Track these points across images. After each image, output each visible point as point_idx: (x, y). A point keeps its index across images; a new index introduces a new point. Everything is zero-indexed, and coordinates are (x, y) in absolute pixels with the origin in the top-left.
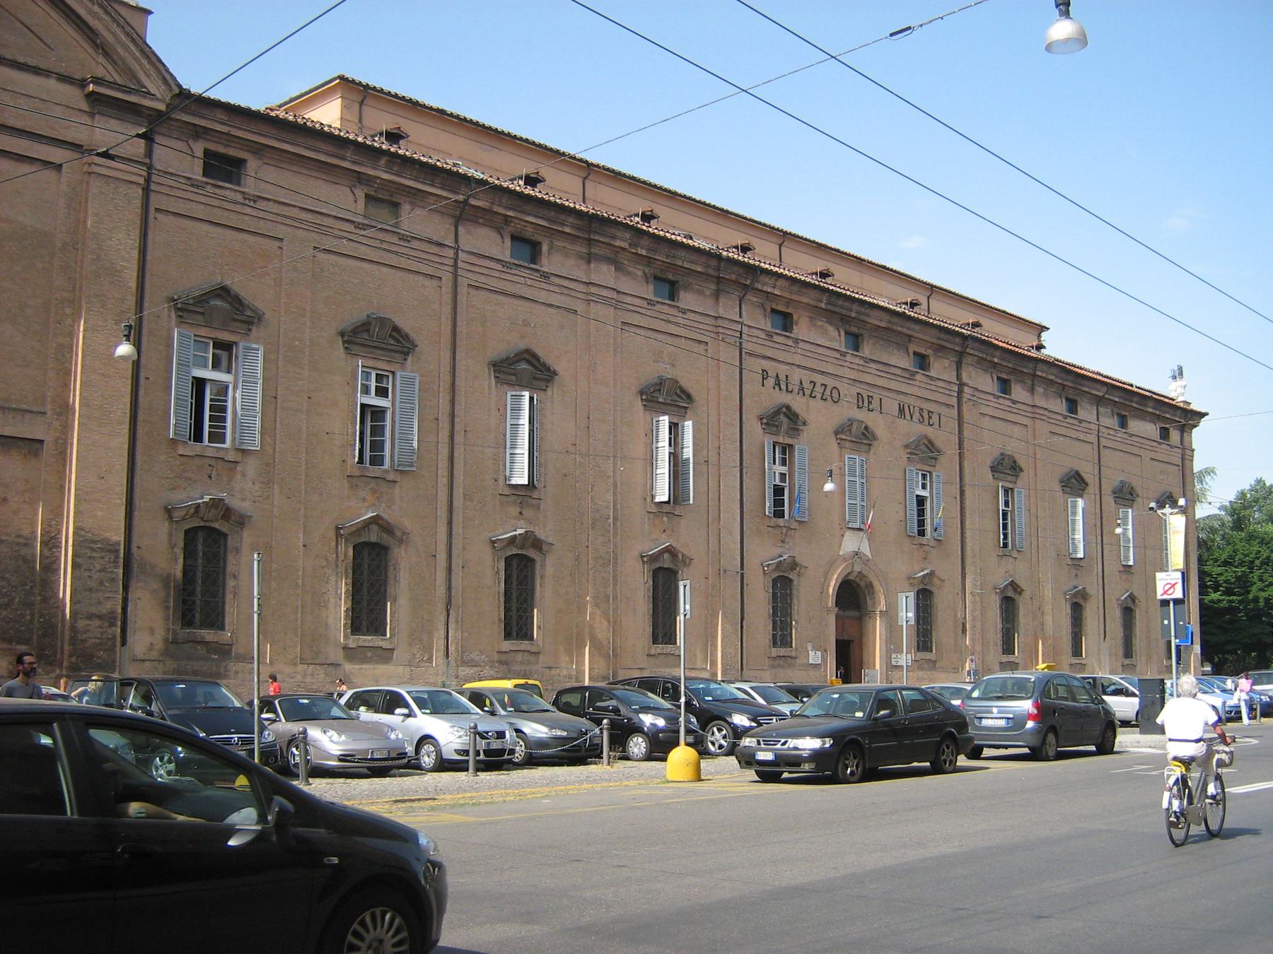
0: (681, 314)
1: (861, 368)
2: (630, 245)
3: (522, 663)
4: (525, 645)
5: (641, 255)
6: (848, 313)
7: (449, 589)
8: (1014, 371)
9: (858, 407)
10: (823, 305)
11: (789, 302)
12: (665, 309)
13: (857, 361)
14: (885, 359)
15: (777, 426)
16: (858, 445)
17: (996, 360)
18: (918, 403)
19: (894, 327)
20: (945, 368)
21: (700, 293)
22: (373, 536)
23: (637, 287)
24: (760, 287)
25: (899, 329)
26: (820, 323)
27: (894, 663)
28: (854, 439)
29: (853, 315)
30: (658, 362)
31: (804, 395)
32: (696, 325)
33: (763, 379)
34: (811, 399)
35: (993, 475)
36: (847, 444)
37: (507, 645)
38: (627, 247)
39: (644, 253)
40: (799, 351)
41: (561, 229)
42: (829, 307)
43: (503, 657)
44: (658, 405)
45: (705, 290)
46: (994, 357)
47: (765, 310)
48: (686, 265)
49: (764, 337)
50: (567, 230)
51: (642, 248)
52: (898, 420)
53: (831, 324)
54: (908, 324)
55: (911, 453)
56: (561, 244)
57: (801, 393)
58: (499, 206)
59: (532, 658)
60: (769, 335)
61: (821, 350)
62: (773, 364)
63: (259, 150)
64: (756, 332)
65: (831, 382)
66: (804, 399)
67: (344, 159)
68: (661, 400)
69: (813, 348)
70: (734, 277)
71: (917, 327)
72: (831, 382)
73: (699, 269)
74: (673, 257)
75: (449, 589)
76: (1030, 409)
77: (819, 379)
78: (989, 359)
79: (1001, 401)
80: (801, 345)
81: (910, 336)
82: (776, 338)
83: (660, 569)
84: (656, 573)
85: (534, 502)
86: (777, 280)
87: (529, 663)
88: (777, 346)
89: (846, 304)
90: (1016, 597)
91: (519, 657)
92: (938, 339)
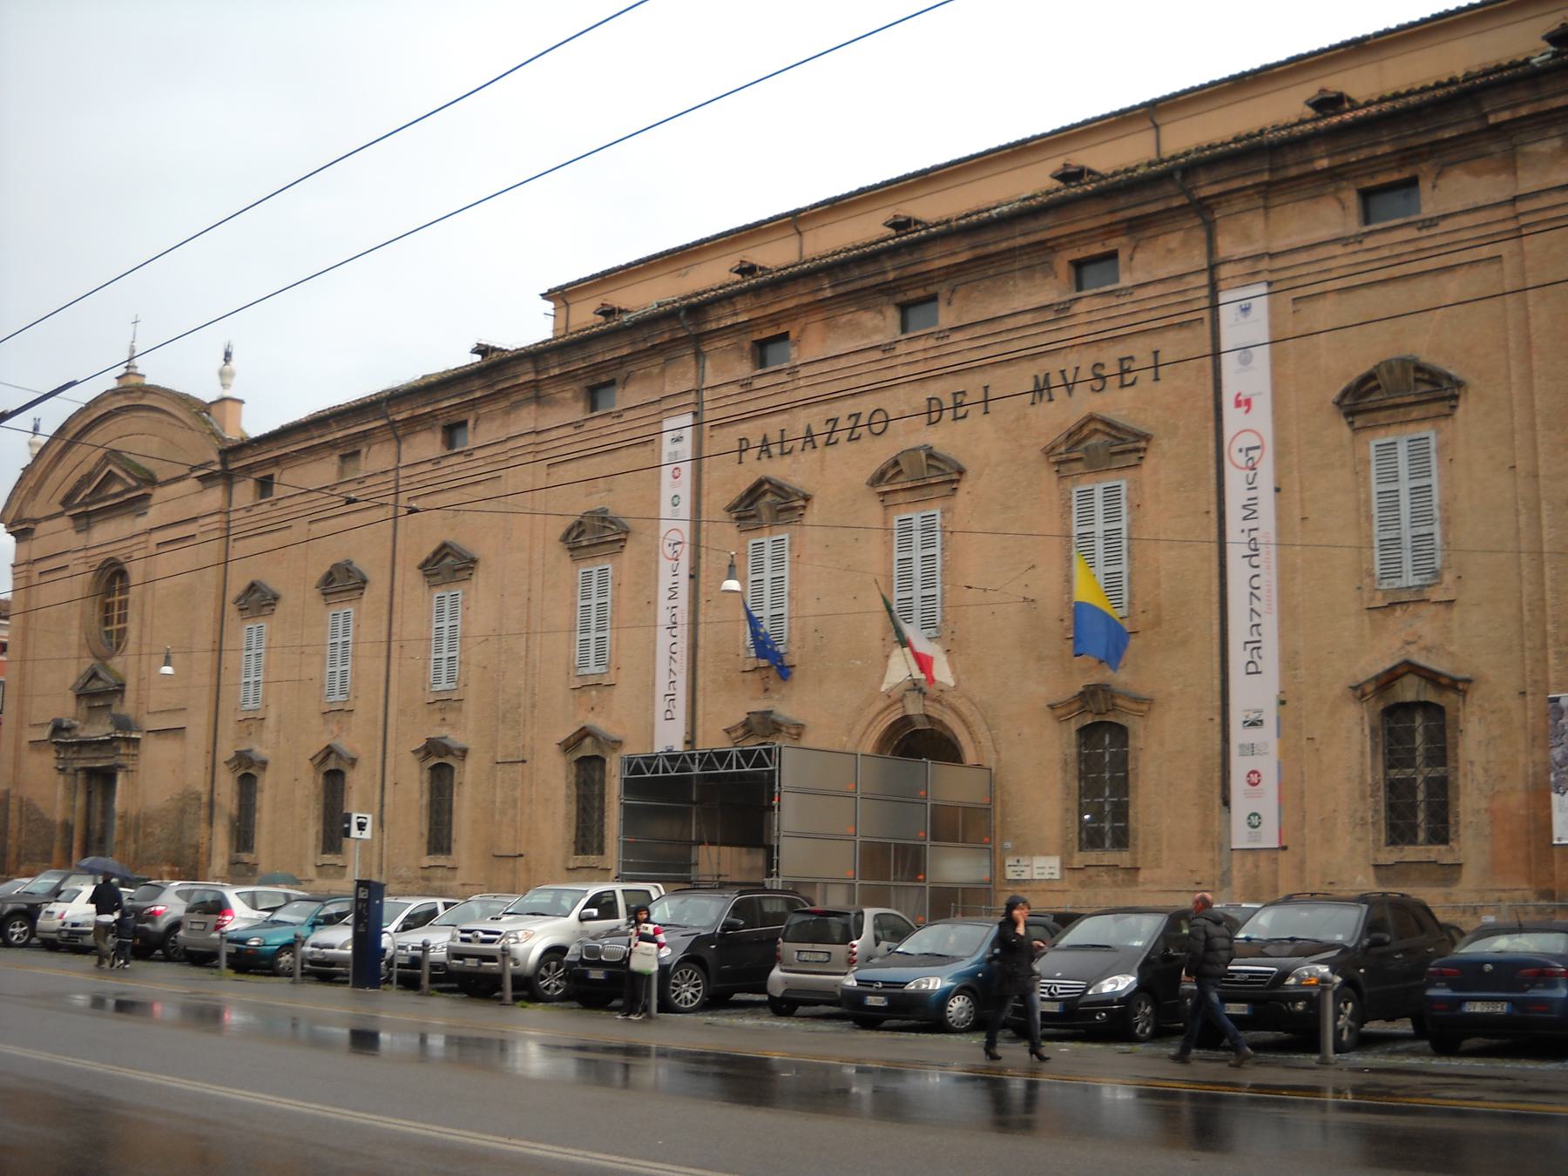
1: (932, 353)
2: (537, 372)
3: (442, 879)
4: (441, 860)
5: (555, 376)
6: (880, 279)
7: (382, 806)
8: (1409, 156)
9: (930, 424)
10: (828, 293)
11: (773, 319)
12: (597, 423)
13: (920, 345)
14: (996, 308)
15: (754, 516)
16: (926, 491)
17: (1324, 163)
18: (1085, 359)
19: (992, 249)
20: (1170, 251)
21: (647, 376)
22: (1409, 690)
23: (568, 409)
24: (714, 326)
25: (1004, 245)
26: (844, 319)
27: (1010, 875)
28: (909, 485)
29: (891, 276)
30: (592, 493)
31: (814, 447)
34: (828, 449)
35: (1351, 423)
36: (900, 498)
37: (427, 861)
38: (531, 377)
39: (557, 371)
40: (802, 383)
41: (471, 397)
42: (841, 290)
43: (426, 873)
44: (585, 550)
46: (1311, 160)
47: (741, 349)
48: (608, 357)
50: (478, 395)
51: (553, 367)
52: (1033, 409)
53: (866, 309)
54: (1019, 228)
55: (1059, 463)
56: (486, 410)
57: (810, 445)
58: (418, 407)
59: (450, 874)
60: (746, 384)
61: (843, 362)
62: (760, 422)
63: (276, 461)
64: (724, 391)
65: (866, 405)
66: (816, 454)
67: (313, 438)
68: (584, 543)
69: (825, 367)
70: (667, 337)
71: (1047, 221)
72: (866, 405)
73: (625, 351)
74: (590, 356)
75: (382, 806)
76: (1505, 212)
77: (843, 410)
78: (1293, 172)
79: (1369, 243)
80: (804, 372)
81: (1042, 242)
82: (758, 383)
83: (584, 758)
84: (583, 762)
85: (457, 704)
86: (734, 304)
87: (447, 879)
88: (762, 393)
89: (871, 268)
90: (1447, 700)
91: (439, 872)
92: (1111, 212)
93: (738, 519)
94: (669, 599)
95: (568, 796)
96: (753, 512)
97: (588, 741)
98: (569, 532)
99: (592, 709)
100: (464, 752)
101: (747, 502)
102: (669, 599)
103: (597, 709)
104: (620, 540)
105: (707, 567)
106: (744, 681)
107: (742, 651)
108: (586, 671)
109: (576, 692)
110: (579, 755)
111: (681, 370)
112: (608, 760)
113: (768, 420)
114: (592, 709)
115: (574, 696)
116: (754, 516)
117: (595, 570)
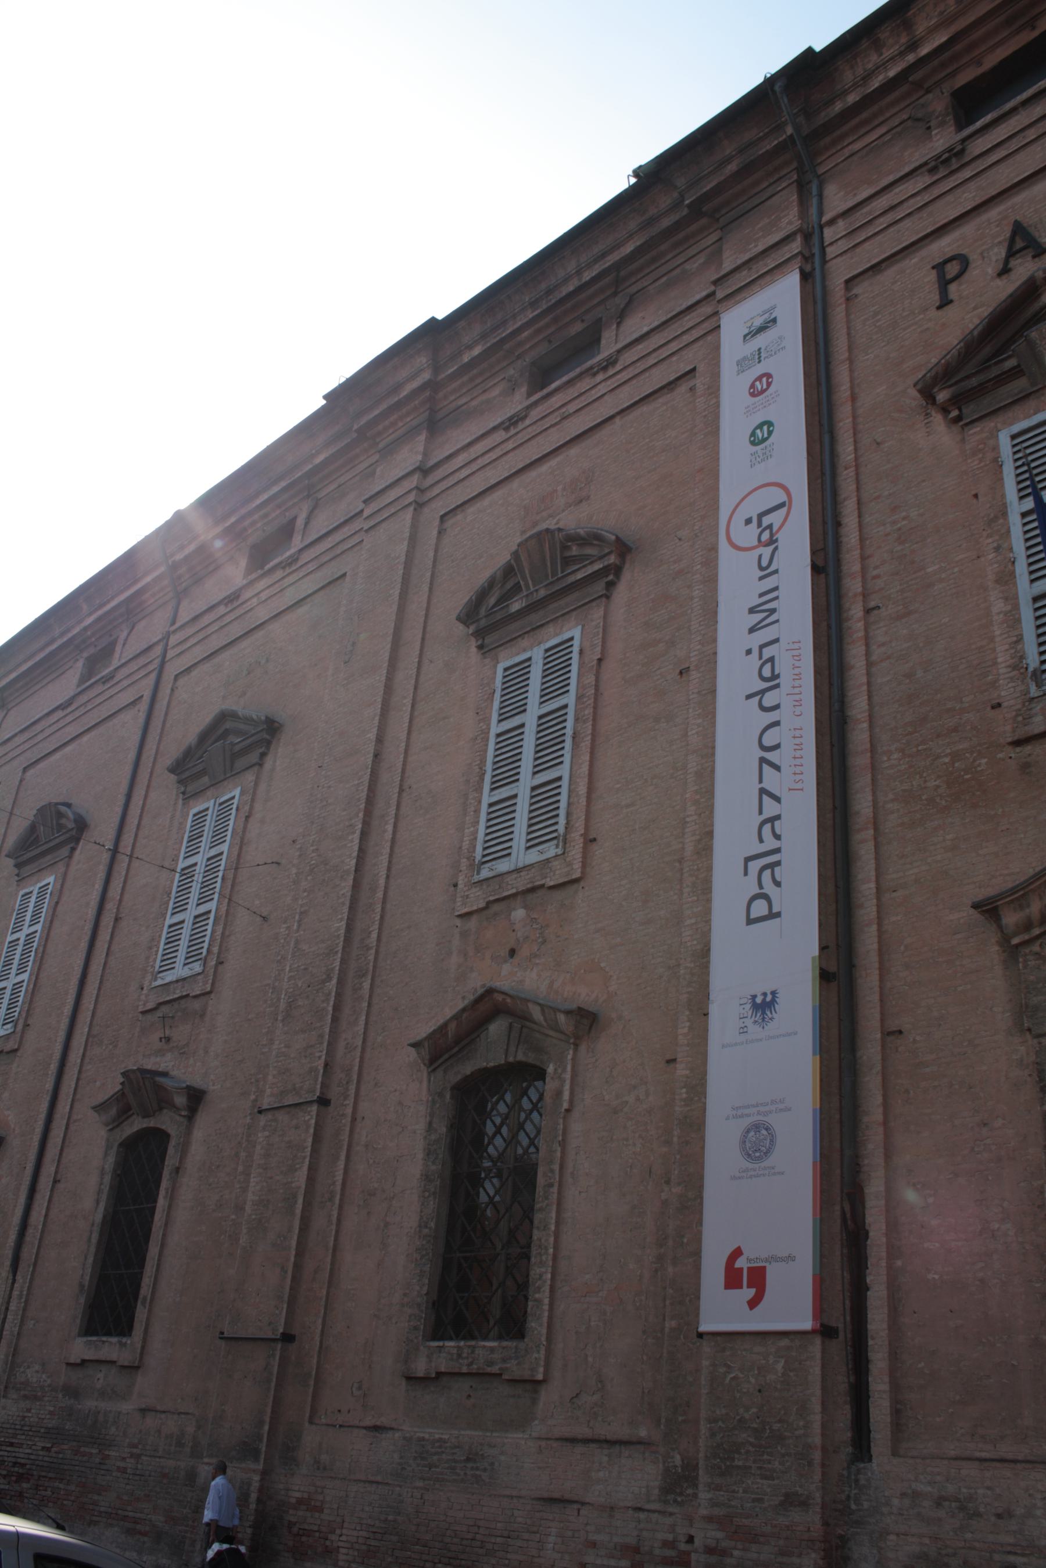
0: (600, 377)
24: (852, 98)
32: (651, 361)
33: (944, 284)
38: (426, 376)
45: (687, 266)
49: (928, 180)
62: (994, 213)
64: (882, 203)
85: (197, 1005)
93: (958, 400)
94: (752, 630)
95: (427, 1178)
96: (1012, 363)
97: (496, 1028)
98: (482, 595)
99: (512, 952)
100: (196, 1097)
101: (987, 350)
102: (752, 630)
103: (524, 952)
104: (605, 571)
105: (862, 540)
106: (1025, 767)
107: (1008, 692)
108: (503, 866)
109: (473, 923)
110: (468, 1068)
111: (766, 221)
112: (550, 1069)
113: (1019, 199)
114: (512, 952)
115: (464, 934)
116: (1016, 372)
117: (537, 654)
